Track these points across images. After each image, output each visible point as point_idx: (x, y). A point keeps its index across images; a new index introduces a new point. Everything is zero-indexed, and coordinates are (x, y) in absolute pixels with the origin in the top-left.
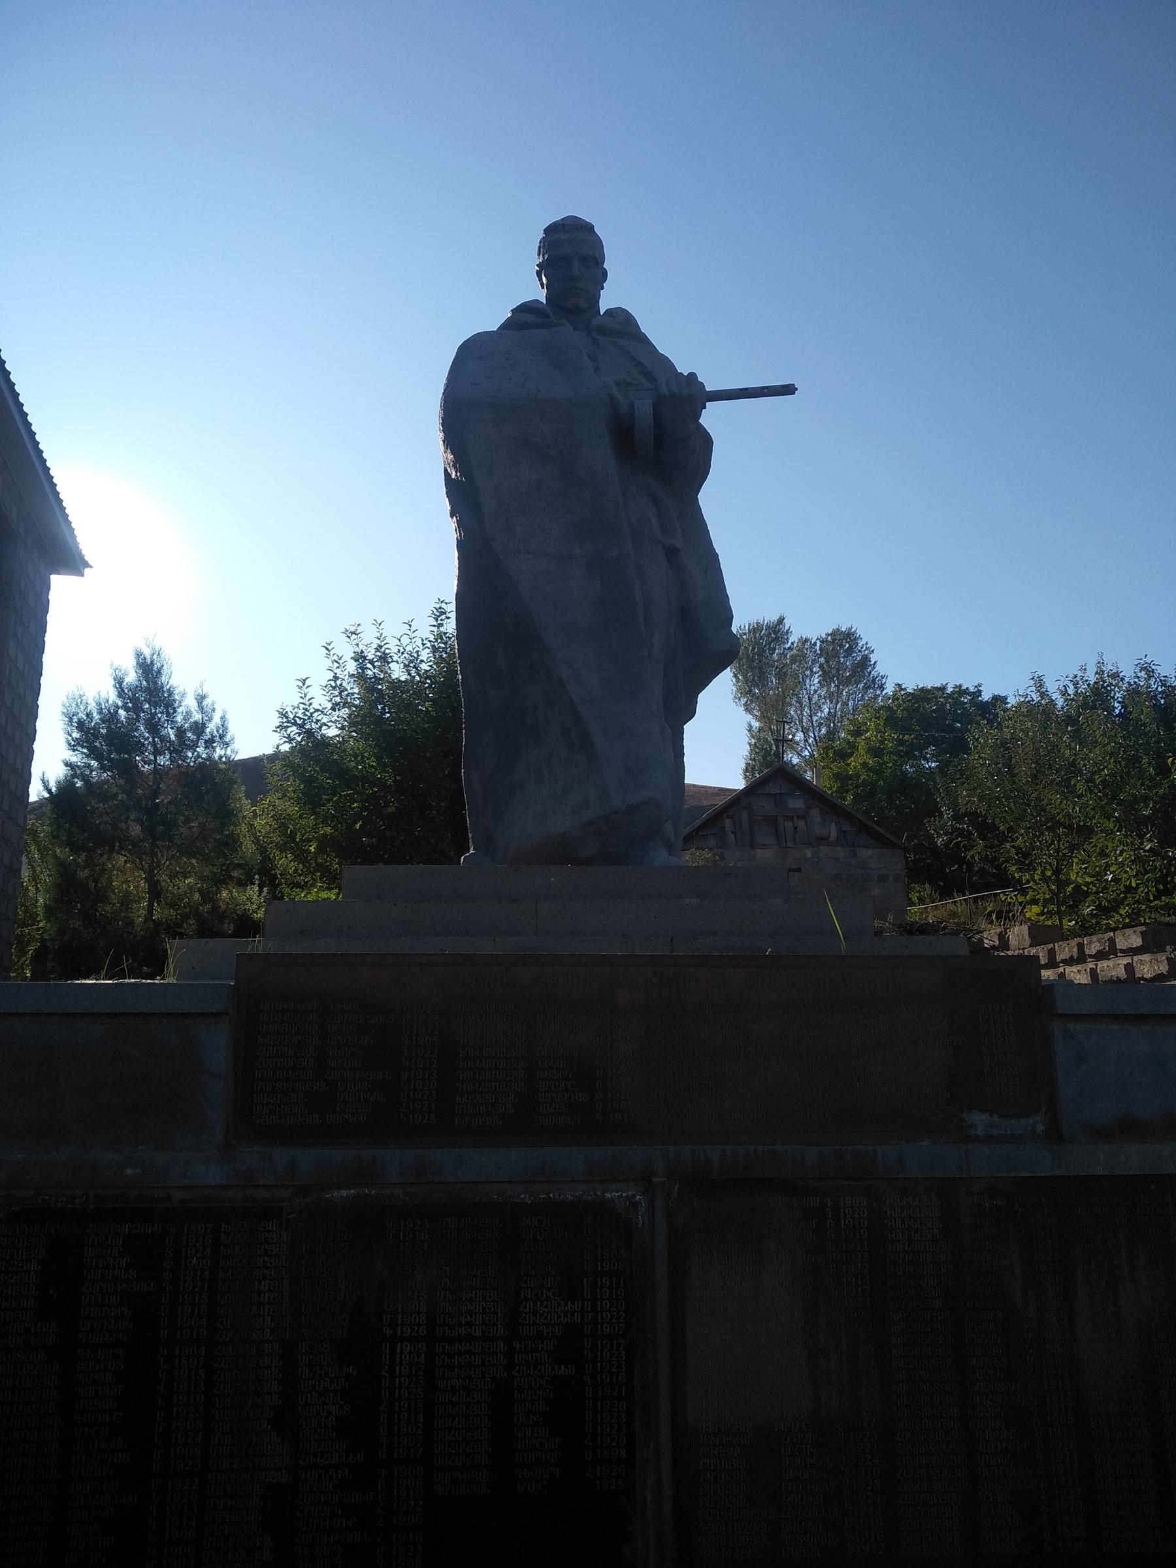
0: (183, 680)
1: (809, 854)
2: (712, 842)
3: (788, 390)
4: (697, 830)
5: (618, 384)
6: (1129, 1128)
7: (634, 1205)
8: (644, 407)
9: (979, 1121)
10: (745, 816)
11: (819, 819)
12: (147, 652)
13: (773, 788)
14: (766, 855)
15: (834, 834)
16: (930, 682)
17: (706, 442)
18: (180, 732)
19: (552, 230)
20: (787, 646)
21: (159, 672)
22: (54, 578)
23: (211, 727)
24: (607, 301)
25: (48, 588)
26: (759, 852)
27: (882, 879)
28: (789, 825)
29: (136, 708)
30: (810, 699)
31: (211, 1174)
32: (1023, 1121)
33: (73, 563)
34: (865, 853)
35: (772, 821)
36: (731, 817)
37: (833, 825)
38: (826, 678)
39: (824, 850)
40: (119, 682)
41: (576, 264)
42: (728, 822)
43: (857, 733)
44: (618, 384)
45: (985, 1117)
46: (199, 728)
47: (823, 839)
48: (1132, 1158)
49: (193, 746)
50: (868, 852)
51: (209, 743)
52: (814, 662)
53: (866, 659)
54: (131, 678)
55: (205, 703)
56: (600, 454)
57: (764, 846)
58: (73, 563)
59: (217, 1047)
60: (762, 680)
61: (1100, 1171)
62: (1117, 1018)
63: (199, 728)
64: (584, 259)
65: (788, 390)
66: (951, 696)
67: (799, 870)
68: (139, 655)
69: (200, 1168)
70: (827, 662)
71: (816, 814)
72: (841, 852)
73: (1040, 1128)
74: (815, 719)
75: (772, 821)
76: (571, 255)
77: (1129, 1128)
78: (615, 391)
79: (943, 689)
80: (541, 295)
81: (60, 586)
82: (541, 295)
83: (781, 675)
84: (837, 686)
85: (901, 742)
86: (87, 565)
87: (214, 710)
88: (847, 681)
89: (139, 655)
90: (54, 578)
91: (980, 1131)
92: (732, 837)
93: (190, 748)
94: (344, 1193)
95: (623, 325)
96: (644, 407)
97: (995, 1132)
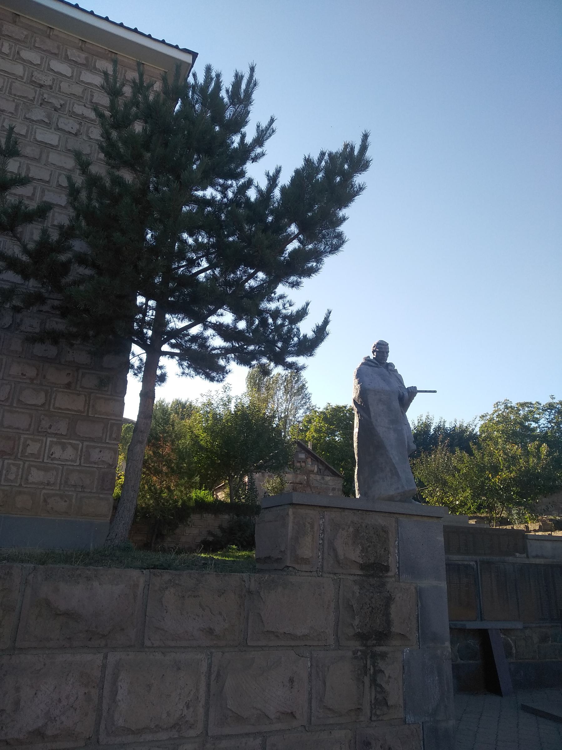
3: (435, 392)
6: (537, 556)
9: (517, 554)
15: (316, 470)
16: (341, 404)
20: (271, 376)
27: (334, 489)
30: (278, 401)
34: (328, 478)
38: (286, 392)
43: (309, 422)
48: (538, 561)
50: (329, 478)
52: (281, 384)
53: (304, 385)
60: (259, 390)
62: (536, 540)
65: (435, 392)
66: (348, 410)
70: (287, 385)
71: (309, 460)
72: (318, 477)
74: (279, 409)
76: (381, 349)
77: (537, 556)
79: (345, 407)
83: (268, 389)
84: (290, 396)
85: (329, 428)
88: (295, 394)
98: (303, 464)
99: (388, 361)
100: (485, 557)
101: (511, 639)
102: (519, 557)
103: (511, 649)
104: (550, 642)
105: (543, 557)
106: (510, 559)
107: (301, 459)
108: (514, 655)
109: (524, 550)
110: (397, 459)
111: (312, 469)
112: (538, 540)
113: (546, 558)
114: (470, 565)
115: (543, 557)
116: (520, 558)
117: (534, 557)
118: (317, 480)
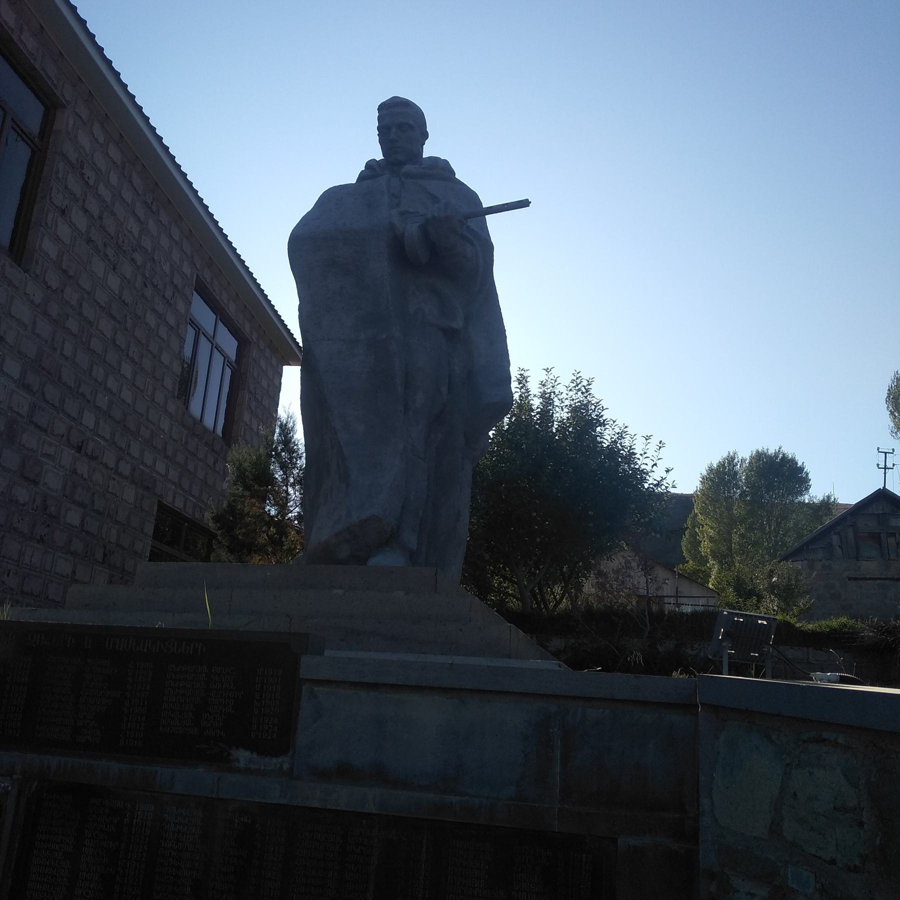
3: (524, 204)
5: (402, 214)
6: (344, 773)
9: (242, 756)
19: (382, 108)
22: (285, 368)
24: (429, 150)
25: (280, 375)
32: (274, 760)
41: (394, 130)
44: (402, 214)
45: (248, 753)
48: (342, 797)
61: (316, 804)
64: (400, 126)
65: (524, 204)
73: (286, 766)
77: (344, 773)
80: (379, 156)
82: (379, 156)
91: (242, 764)
95: (441, 170)
96: (412, 229)
97: (253, 767)
99: (425, 155)
106: (187, 778)
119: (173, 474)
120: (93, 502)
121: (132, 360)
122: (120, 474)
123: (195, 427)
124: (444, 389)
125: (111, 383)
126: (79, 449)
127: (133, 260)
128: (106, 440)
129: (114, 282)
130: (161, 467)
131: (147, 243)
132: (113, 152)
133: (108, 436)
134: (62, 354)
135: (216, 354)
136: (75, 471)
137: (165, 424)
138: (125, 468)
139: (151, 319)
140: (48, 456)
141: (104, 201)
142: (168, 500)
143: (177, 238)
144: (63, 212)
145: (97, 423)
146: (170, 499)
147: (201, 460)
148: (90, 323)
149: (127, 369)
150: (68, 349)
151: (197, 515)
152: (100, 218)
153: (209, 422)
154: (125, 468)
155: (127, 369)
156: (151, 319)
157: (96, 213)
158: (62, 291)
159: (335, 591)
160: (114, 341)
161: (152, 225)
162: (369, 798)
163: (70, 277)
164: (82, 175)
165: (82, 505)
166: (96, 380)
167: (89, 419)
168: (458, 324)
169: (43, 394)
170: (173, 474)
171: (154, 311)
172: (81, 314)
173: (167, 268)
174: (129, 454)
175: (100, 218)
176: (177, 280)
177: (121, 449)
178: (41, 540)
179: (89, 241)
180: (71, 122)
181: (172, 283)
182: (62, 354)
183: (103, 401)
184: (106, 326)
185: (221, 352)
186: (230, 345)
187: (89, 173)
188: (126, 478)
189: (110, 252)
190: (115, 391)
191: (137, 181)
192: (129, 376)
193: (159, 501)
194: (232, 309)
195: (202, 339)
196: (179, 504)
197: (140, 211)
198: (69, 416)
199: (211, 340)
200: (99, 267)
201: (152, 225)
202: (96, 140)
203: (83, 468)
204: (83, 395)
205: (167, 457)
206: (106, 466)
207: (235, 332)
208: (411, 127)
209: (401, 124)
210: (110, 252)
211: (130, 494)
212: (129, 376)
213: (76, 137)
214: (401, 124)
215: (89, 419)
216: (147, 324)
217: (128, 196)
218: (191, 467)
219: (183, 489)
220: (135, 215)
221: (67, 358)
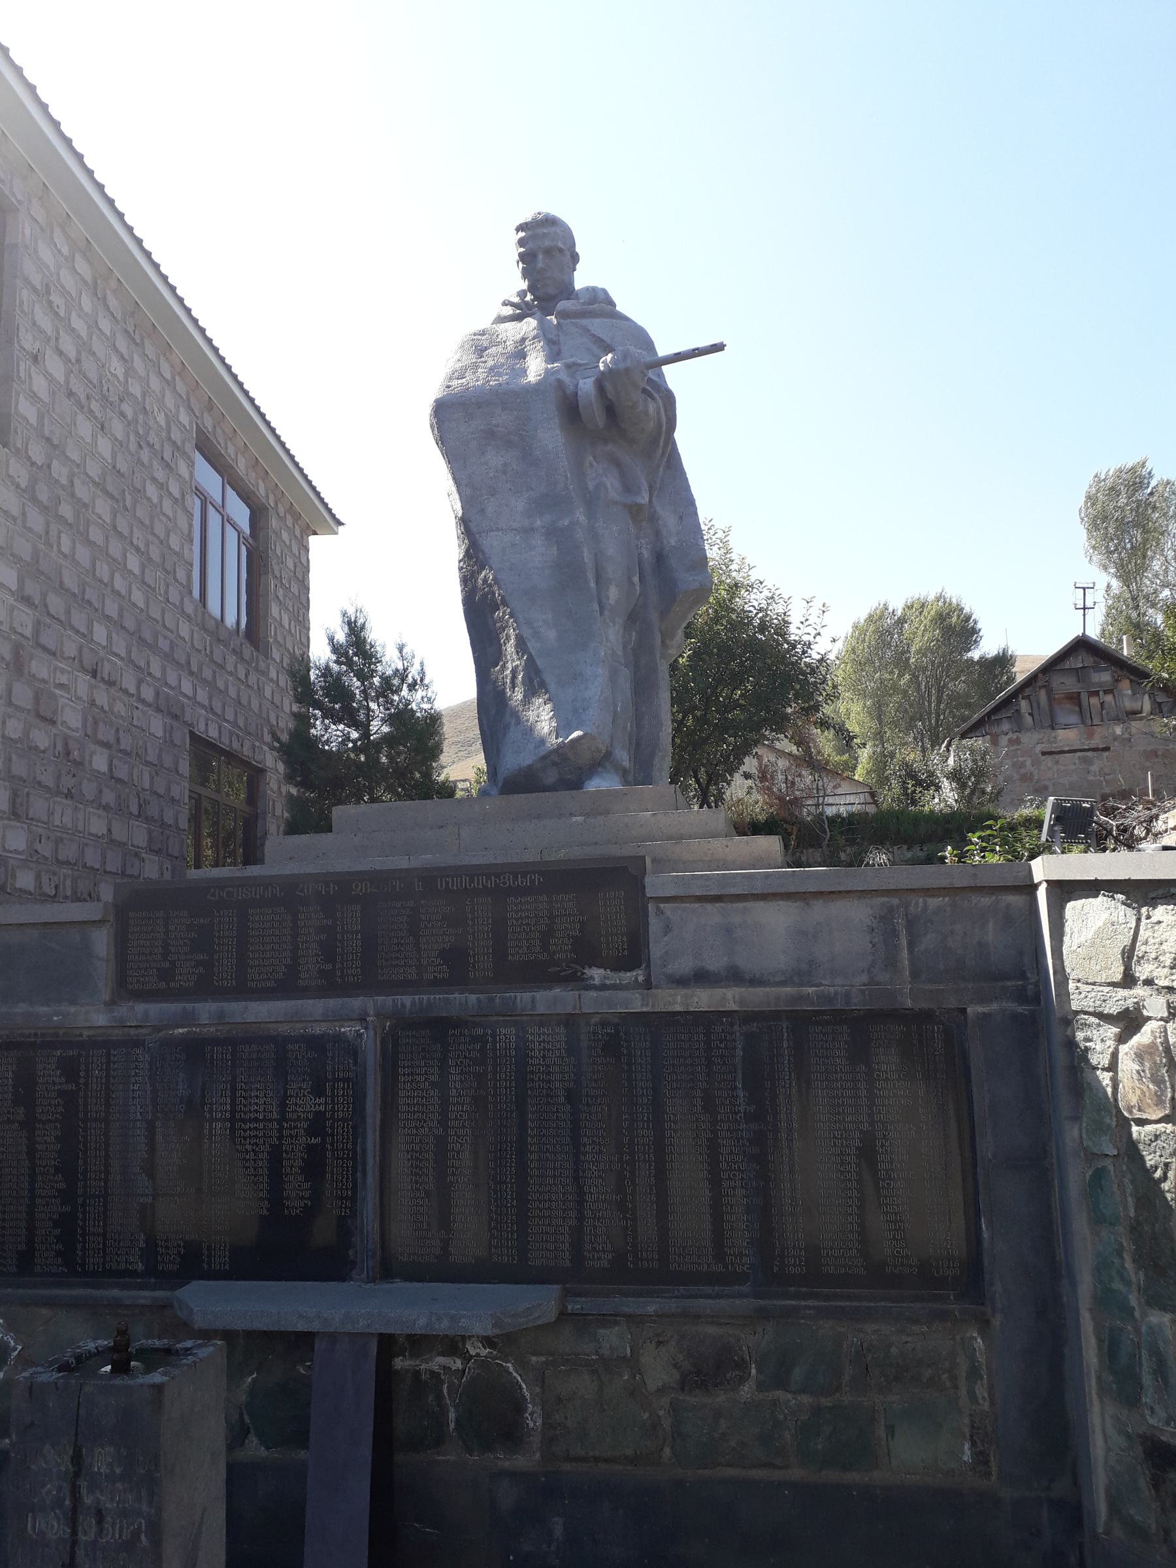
0: (380, 636)
1: (1118, 730)
2: (1006, 726)
3: (718, 348)
4: (989, 714)
6: (701, 977)
7: (360, 1036)
8: (587, 385)
9: (597, 974)
10: (1043, 694)
11: (1130, 692)
12: (351, 612)
13: (1076, 662)
14: (1068, 737)
15: (1147, 706)
17: (669, 400)
18: (386, 680)
21: (363, 627)
22: (313, 540)
23: (414, 673)
24: (582, 279)
26: (1061, 734)
28: (1094, 701)
29: (349, 663)
31: (100, 1019)
32: (629, 974)
33: (330, 522)
35: (1075, 698)
36: (1028, 698)
37: (1146, 697)
39: (1136, 726)
40: (331, 639)
41: (540, 257)
42: (1024, 705)
45: (601, 971)
46: (402, 675)
47: (1133, 714)
48: (703, 999)
49: (398, 691)
51: (412, 687)
54: (341, 637)
55: (405, 651)
56: (551, 437)
57: (1066, 727)
58: (330, 522)
59: (102, 942)
61: (678, 1008)
63: (402, 675)
64: (548, 252)
65: (718, 348)
67: (1107, 749)
68: (344, 614)
69: (93, 1016)
71: (1125, 687)
73: (641, 978)
75: (1075, 698)
77: (701, 977)
78: (564, 377)
81: (317, 544)
86: (340, 523)
87: (413, 657)
89: (344, 614)
90: (313, 540)
91: (597, 982)
92: (1029, 719)
93: (393, 692)
94: (181, 1031)
95: (599, 303)
97: (608, 982)
98: (1109, 698)
100: (407, 1000)
101: (522, 1365)
102: (603, 987)
103: (518, 1406)
104: (747, 1391)
105: (735, 976)
107: (1100, 684)
108: (536, 1439)
109: (633, 954)
110: (552, 634)
111: (1136, 706)
112: (718, 899)
113: (755, 981)
114: (338, 1038)
115: (735, 976)
116: (609, 994)
117: (681, 982)
118: (1152, 735)
119: (202, 696)
120: (118, 741)
121: (138, 549)
122: (143, 701)
123: (215, 629)
124: (636, 579)
125: (119, 584)
126: (94, 673)
127: (122, 414)
128: (122, 659)
129: (104, 447)
130: (187, 687)
131: (135, 389)
132: (82, 266)
133: (123, 654)
134: (59, 551)
135: (228, 527)
136: (93, 703)
137: (185, 629)
138: (148, 694)
139: (152, 491)
140: (61, 686)
141: (79, 336)
142: (200, 729)
143: (168, 376)
144: (35, 359)
145: (109, 638)
146: (202, 727)
147: (231, 674)
148: (85, 505)
149: (133, 563)
150: (66, 542)
151: (236, 746)
152: (78, 361)
153: (230, 620)
154: (148, 694)
155: (133, 563)
156: (152, 491)
157: (72, 354)
158: (49, 467)
159: (574, 819)
160: (115, 527)
161: (138, 364)
162: (730, 998)
163: (55, 447)
164: (50, 303)
165: (106, 745)
166: (101, 581)
167: (100, 633)
168: (643, 499)
169: (46, 605)
170: (202, 696)
171: (154, 479)
172: (73, 495)
173: (161, 419)
174: (150, 674)
175: (78, 361)
176: (176, 435)
177: (139, 668)
178: (69, 795)
179: (71, 394)
180: (28, 231)
181: (170, 439)
182: (59, 551)
183: (112, 609)
184: (103, 507)
185: (234, 526)
186: (240, 513)
187: (57, 300)
188: (149, 705)
189: (95, 406)
190: (123, 593)
191: (113, 302)
192: (137, 571)
193: (191, 732)
194: (241, 466)
195: (210, 509)
196: (213, 733)
197: (122, 344)
198: (77, 632)
199: (221, 510)
200: (85, 428)
201: (138, 364)
202: (60, 252)
203: (102, 698)
204: (89, 603)
205: (191, 673)
206: (126, 692)
207: (246, 497)
208: (561, 251)
209: (546, 250)
210: (95, 406)
211: (157, 725)
212: (137, 571)
213: (36, 251)
214: (546, 250)
215: (100, 633)
216: (149, 499)
217: (106, 325)
218: (220, 684)
219: (215, 714)
220: (117, 351)
221: (65, 556)
